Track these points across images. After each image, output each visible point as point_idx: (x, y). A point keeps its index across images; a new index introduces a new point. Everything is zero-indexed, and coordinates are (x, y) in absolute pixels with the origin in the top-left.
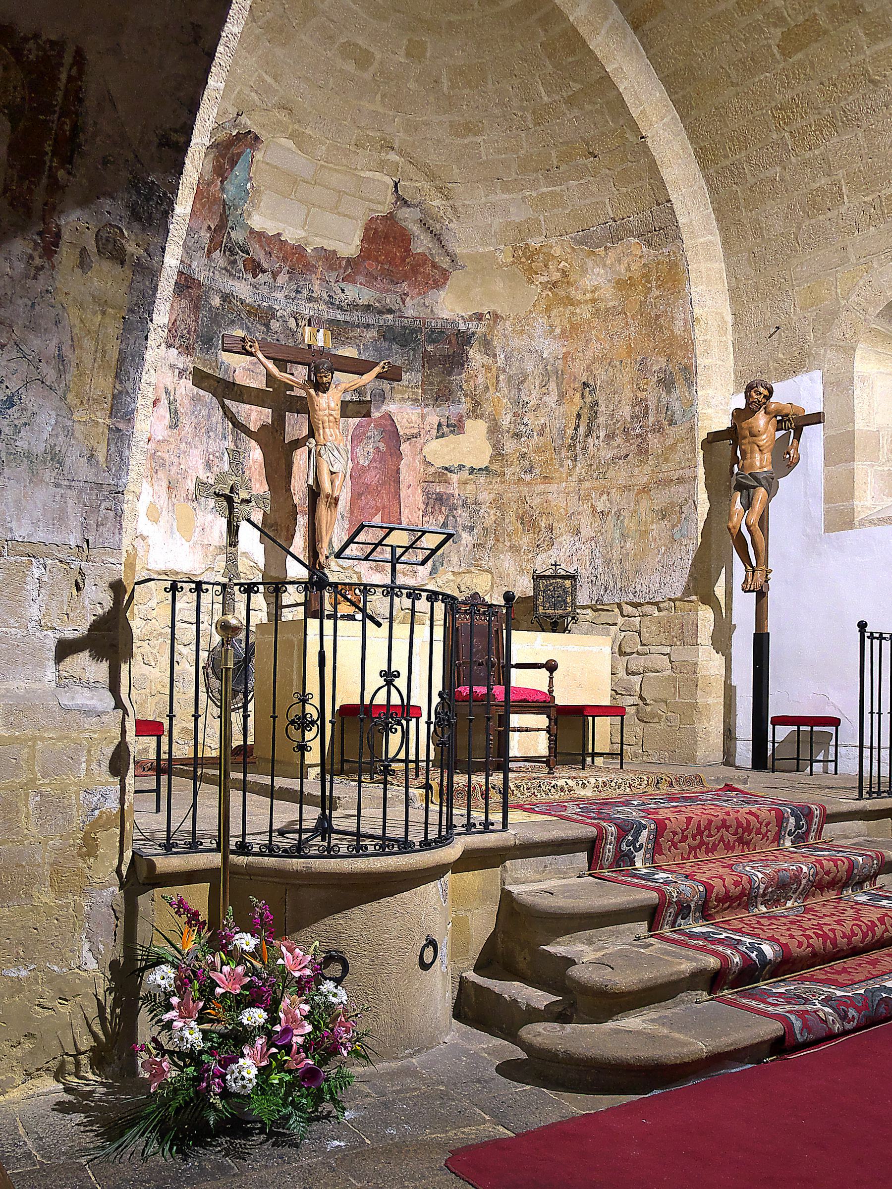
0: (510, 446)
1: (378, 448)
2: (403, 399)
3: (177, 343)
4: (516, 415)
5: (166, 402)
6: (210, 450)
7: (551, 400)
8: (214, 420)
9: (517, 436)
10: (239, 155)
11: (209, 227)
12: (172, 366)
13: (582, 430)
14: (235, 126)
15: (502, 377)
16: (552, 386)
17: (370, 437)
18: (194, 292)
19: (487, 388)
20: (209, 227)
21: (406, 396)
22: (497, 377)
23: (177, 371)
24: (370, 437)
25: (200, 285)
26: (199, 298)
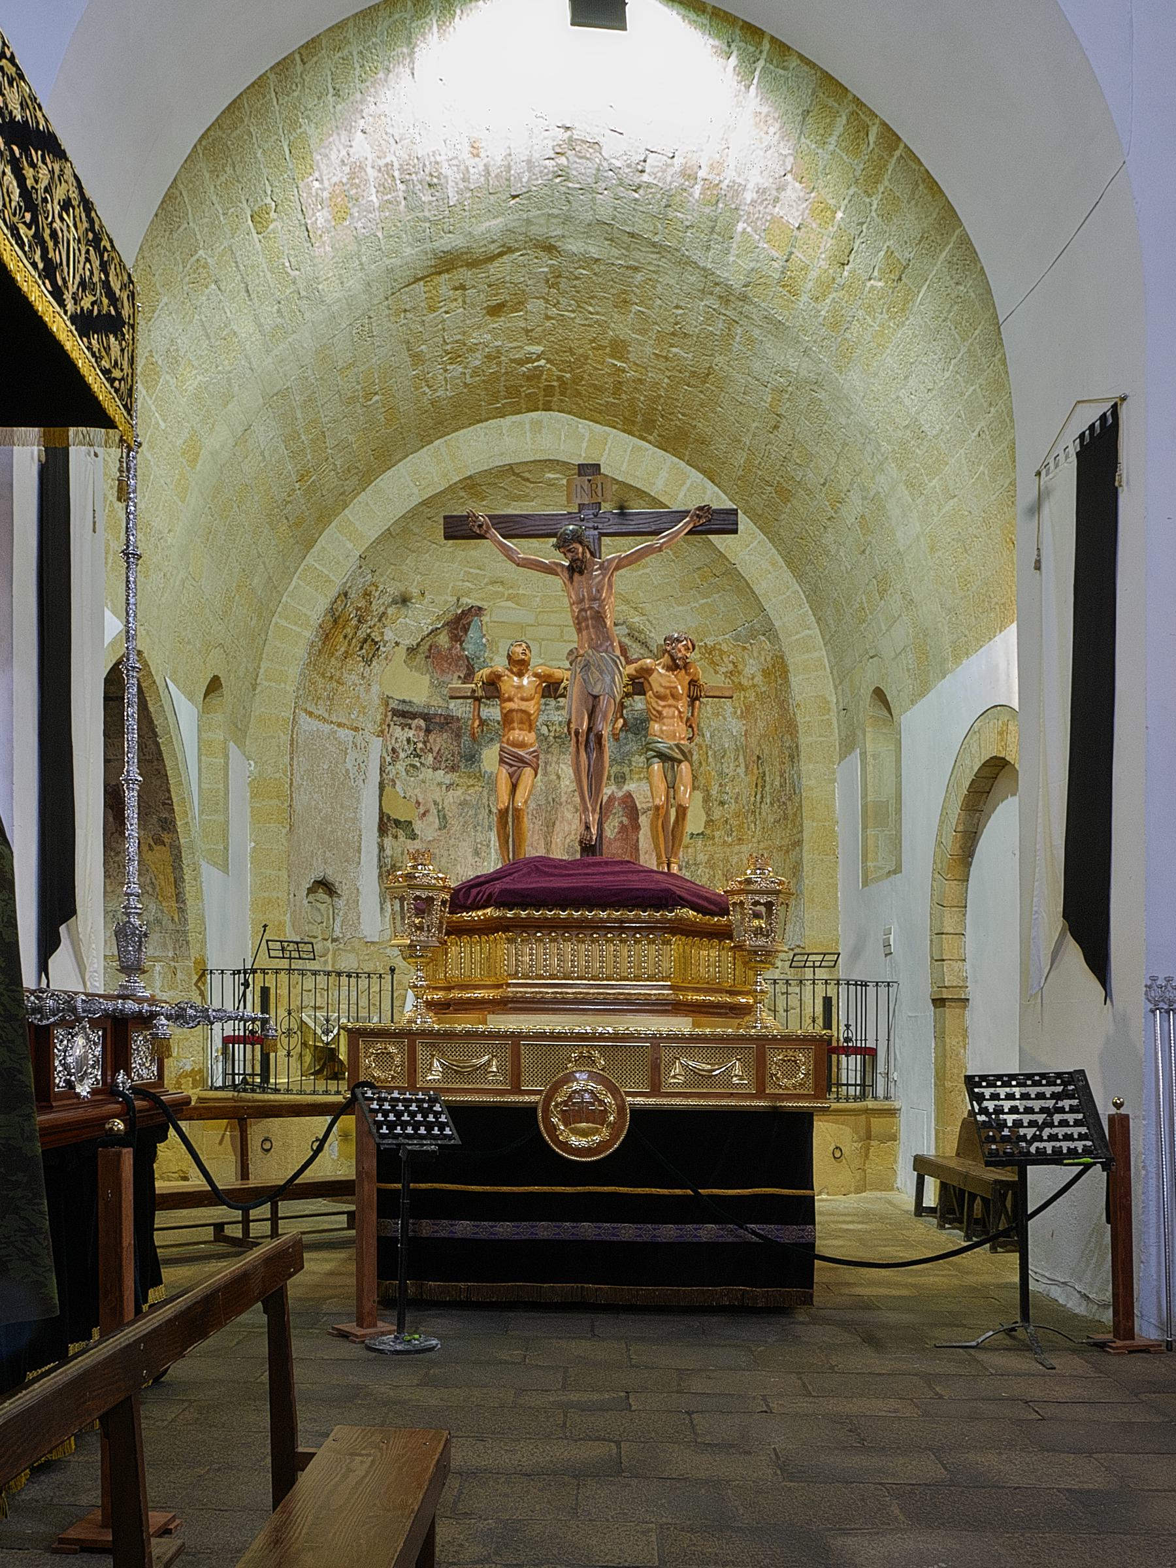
0: (717, 813)
1: (622, 822)
2: (640, 779)
3: (443, 765)
4: (721, 785)
5: (435, 811)
6: (478, 841)
7: (741, 770)
8: (481, 817)
9: (722, 803)
10: (469, 624)
11: (459, 677)
12: (439, 784)
13: (758, 797)
14: (459, 607)
15: (710, 753)
16: (741, 758)
17: (615, 814)
18: (454, 726)
19: (700, 763)
20: (459, 677)
21: (642, 776)
22: (707, 753)
23: (444, 786)
24: (615, 814)
25: (458, 719)
26: (460, 728)
